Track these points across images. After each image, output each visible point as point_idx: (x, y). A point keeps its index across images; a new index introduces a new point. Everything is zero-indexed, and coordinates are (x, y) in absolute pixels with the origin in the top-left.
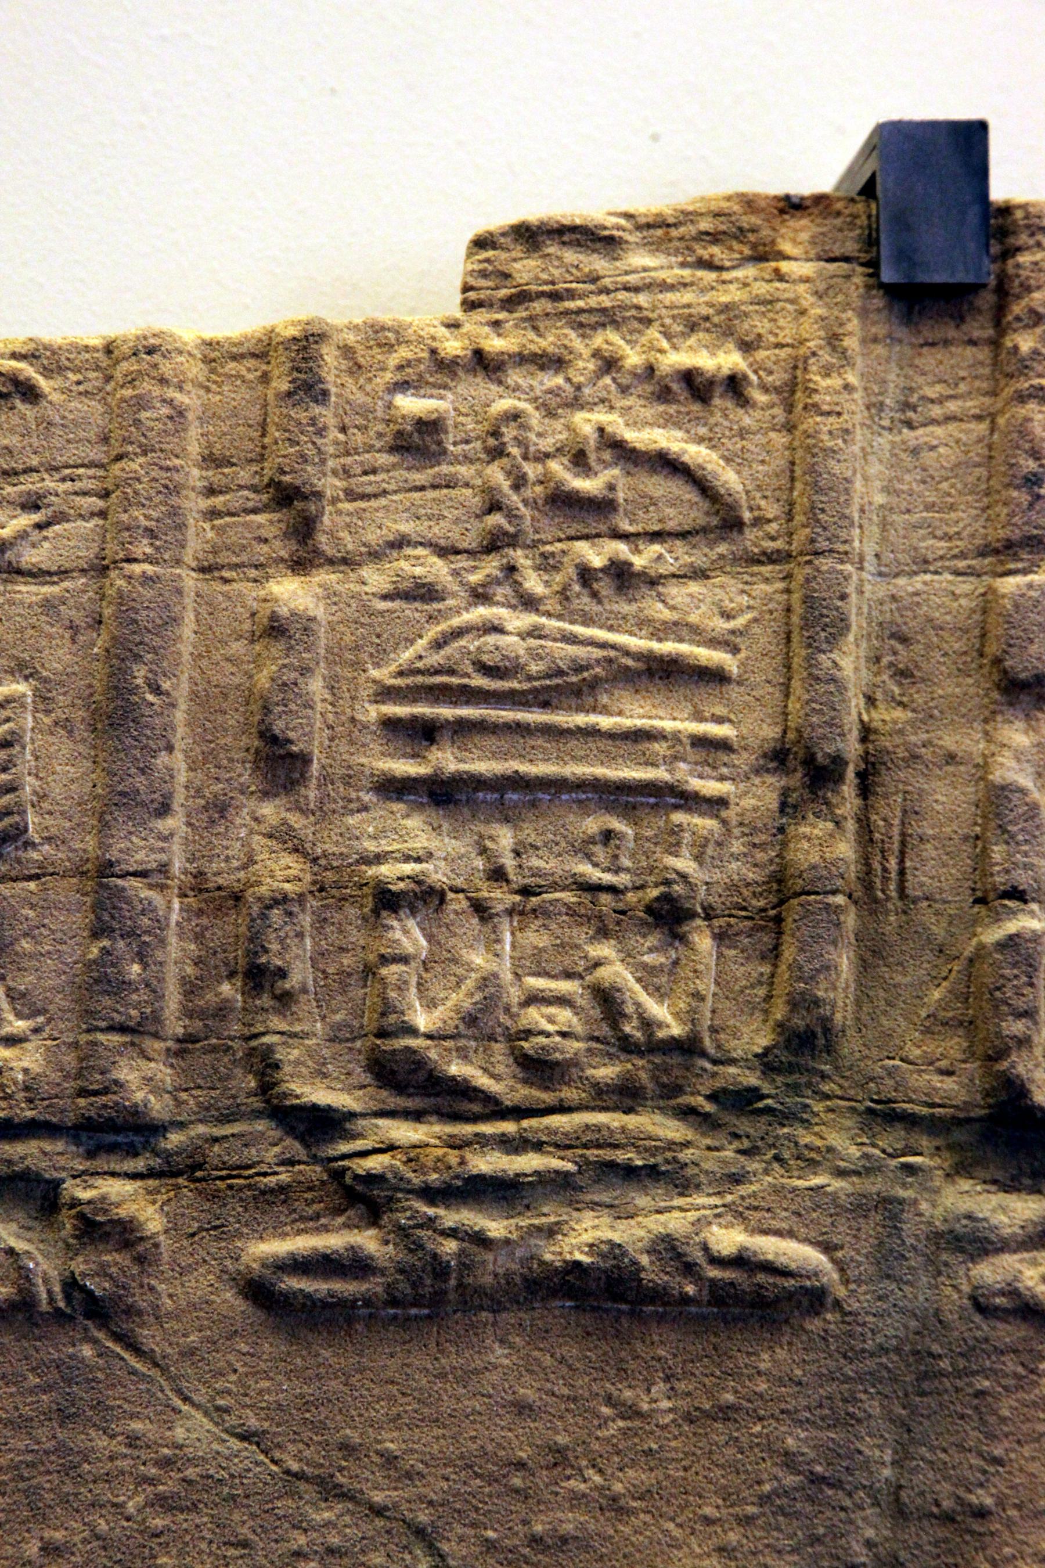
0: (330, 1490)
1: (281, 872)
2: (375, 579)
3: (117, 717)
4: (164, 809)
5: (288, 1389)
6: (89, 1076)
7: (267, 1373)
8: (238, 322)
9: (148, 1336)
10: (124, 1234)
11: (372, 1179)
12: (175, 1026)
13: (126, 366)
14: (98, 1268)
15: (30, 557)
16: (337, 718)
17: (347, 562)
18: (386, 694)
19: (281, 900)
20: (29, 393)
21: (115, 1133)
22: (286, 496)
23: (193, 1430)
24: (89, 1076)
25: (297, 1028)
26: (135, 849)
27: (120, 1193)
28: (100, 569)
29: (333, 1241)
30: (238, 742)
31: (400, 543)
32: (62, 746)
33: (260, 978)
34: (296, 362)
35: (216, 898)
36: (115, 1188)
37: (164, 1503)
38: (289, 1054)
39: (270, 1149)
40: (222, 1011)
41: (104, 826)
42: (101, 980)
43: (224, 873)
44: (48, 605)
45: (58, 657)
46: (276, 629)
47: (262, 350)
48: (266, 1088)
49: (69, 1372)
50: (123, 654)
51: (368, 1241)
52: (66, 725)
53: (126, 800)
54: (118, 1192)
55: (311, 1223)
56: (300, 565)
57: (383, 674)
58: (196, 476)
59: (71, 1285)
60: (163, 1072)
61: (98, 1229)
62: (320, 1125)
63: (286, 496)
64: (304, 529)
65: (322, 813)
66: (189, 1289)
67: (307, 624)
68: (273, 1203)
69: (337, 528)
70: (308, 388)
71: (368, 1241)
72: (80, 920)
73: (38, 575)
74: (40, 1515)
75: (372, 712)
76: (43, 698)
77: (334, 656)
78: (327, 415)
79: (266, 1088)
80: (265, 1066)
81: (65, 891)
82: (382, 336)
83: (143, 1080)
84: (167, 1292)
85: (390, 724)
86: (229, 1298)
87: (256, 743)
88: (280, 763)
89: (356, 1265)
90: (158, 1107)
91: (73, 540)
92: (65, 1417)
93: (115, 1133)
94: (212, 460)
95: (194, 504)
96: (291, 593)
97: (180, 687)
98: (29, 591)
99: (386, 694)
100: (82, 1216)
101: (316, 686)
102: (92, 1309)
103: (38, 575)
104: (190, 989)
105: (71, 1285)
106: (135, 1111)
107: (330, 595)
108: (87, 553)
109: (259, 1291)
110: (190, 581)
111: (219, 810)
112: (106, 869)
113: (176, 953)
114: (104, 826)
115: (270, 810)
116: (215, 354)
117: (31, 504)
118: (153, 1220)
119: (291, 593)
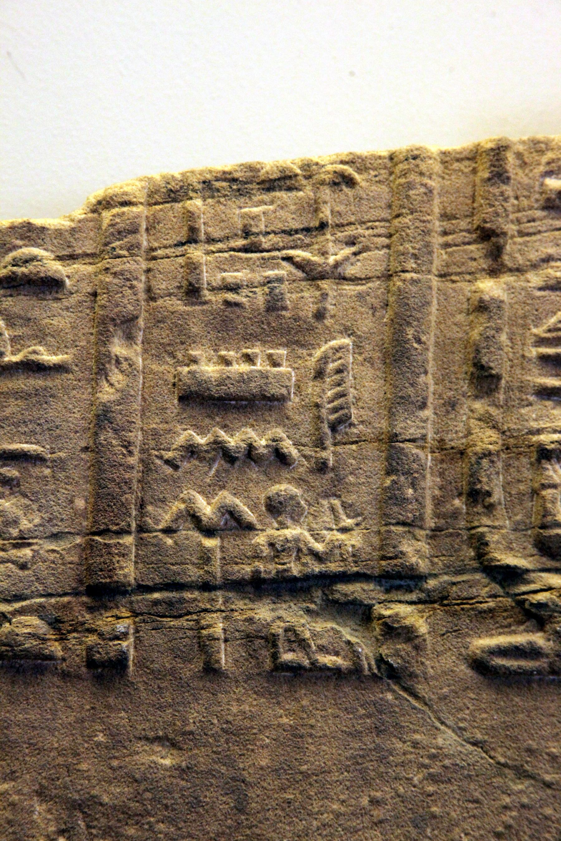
0: (521, 773)
1: (487, 439)
2: (535, 279)
3: (397, 356)
4: (423, 406)
5: (498, 718)
6: (386, 549)
7: (486, 709)
8: (458, 142)
9: (421, 689)
10: (409, 634)
11: (540, 605)
12: (431, 523)
13: (401, 167)
14: (395, 652)
15: (350, 270)
16: (515, 355)
17: (519, 270)
18: (541, 341)
19: (488, 454)
20: (350, 182)
21: (401, 579)
22: (487, 235)
23: (447, 739)
24: (386, 549)
25: (497, 524)
26: (408, 426)
27: (404, 611)
28: (388, 276)
29: (520, 639)
30: (461, 369)
31: (548, 259)
32: (368, 372)
33: (476, 496)
34: (493, 162)
35: (450, 454)
36: (403, 609)
37: (433, 778)
38: (493, 538)
39: (483, 589)
40: (455, 514)
41: (391, 415)
42: (391, 498)
43: (455, 440)
44: (360, 296)
45: (366, 324)
46: (482, 307)
47: (473, 156)
48: (480, 556)
49: (380, 708)
50: (400, 322)
51: (538, 639)
52: (370, 361)
53: (401, 401)
54: (404, 611)
55: (506, 629)
56: (493, 273)
57: (539, 331)
58: (438, 225)
59: (380, 660)
60: (424, 546)
61: (393, 631)
62: (510, 576)
63: (487, 235)
64: (496, 253)
65: (507, 407)
66: (442, 664)
67: (499, 304)
68: (486, 618)
69: (513, 251)
70: (499, 176)
71: (538, 639)
72: (379, 466)
73: (355, 280)
74: (368, 783)
75: (534, 352)
76: (357, 346)
77: (512, 322)
78: (508, 190)
79: (480, 556)
80: (480, 544)
81: (371, 450)
82: (538, 146)
83: (415, 551)
84: (430, 665)
85: (544, 359)
86: (463, 669)
87: (472, 369)
88: (484, 380)
89: (532, 652)
90: (423, 566)
91: (373, 261)
92: (379, 731)
93: (401, 579)
94: (445, 216)
95: (437, 240)
96: (490, 287)
97: (430, 339)
98: (350, 289)
99: (541, 341)
100: (385, 624)
101: (503, 338)
102: (391, 673)
103: (355, 280)
104: (438, 502)
105: (380, 660)
106: (412, 568)
107: (510, 288)
108: (380, 268)
109: (480, 665)
110: (435, 282)
111: (451, 405)
112: (393, 438)
113: (430, 483)
114: (391, 415)
115: (478, 405)
116: (447, 159)
117: (351, 242)
118: (423, 627)
119: (490, 287)
